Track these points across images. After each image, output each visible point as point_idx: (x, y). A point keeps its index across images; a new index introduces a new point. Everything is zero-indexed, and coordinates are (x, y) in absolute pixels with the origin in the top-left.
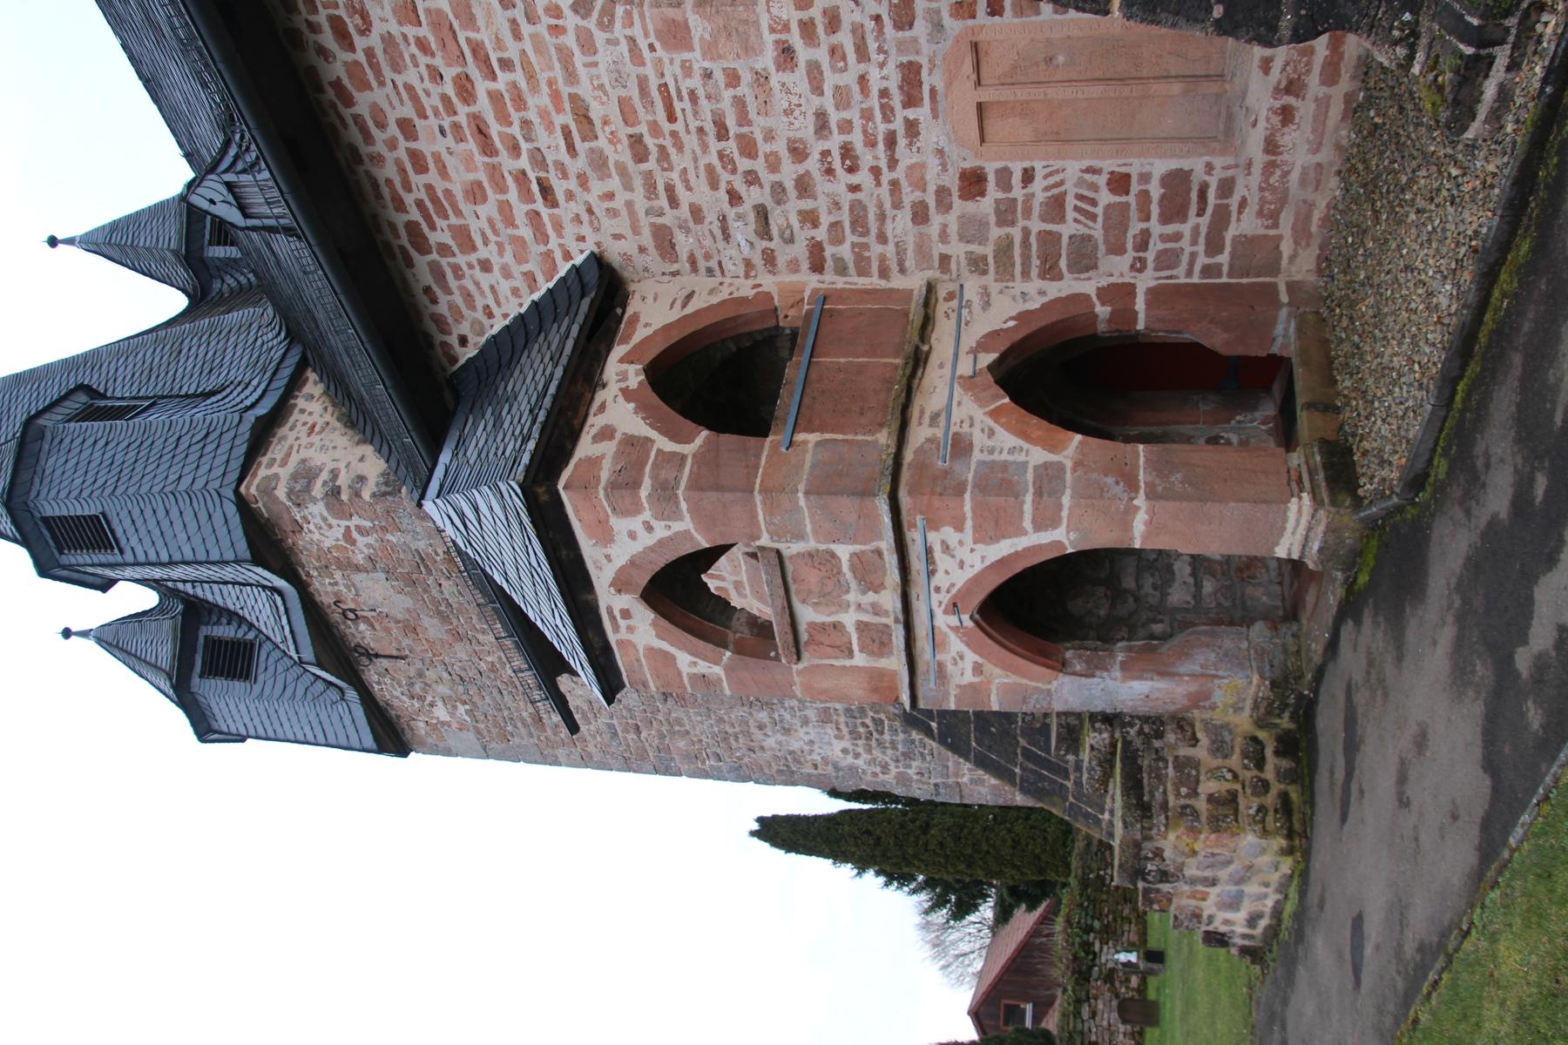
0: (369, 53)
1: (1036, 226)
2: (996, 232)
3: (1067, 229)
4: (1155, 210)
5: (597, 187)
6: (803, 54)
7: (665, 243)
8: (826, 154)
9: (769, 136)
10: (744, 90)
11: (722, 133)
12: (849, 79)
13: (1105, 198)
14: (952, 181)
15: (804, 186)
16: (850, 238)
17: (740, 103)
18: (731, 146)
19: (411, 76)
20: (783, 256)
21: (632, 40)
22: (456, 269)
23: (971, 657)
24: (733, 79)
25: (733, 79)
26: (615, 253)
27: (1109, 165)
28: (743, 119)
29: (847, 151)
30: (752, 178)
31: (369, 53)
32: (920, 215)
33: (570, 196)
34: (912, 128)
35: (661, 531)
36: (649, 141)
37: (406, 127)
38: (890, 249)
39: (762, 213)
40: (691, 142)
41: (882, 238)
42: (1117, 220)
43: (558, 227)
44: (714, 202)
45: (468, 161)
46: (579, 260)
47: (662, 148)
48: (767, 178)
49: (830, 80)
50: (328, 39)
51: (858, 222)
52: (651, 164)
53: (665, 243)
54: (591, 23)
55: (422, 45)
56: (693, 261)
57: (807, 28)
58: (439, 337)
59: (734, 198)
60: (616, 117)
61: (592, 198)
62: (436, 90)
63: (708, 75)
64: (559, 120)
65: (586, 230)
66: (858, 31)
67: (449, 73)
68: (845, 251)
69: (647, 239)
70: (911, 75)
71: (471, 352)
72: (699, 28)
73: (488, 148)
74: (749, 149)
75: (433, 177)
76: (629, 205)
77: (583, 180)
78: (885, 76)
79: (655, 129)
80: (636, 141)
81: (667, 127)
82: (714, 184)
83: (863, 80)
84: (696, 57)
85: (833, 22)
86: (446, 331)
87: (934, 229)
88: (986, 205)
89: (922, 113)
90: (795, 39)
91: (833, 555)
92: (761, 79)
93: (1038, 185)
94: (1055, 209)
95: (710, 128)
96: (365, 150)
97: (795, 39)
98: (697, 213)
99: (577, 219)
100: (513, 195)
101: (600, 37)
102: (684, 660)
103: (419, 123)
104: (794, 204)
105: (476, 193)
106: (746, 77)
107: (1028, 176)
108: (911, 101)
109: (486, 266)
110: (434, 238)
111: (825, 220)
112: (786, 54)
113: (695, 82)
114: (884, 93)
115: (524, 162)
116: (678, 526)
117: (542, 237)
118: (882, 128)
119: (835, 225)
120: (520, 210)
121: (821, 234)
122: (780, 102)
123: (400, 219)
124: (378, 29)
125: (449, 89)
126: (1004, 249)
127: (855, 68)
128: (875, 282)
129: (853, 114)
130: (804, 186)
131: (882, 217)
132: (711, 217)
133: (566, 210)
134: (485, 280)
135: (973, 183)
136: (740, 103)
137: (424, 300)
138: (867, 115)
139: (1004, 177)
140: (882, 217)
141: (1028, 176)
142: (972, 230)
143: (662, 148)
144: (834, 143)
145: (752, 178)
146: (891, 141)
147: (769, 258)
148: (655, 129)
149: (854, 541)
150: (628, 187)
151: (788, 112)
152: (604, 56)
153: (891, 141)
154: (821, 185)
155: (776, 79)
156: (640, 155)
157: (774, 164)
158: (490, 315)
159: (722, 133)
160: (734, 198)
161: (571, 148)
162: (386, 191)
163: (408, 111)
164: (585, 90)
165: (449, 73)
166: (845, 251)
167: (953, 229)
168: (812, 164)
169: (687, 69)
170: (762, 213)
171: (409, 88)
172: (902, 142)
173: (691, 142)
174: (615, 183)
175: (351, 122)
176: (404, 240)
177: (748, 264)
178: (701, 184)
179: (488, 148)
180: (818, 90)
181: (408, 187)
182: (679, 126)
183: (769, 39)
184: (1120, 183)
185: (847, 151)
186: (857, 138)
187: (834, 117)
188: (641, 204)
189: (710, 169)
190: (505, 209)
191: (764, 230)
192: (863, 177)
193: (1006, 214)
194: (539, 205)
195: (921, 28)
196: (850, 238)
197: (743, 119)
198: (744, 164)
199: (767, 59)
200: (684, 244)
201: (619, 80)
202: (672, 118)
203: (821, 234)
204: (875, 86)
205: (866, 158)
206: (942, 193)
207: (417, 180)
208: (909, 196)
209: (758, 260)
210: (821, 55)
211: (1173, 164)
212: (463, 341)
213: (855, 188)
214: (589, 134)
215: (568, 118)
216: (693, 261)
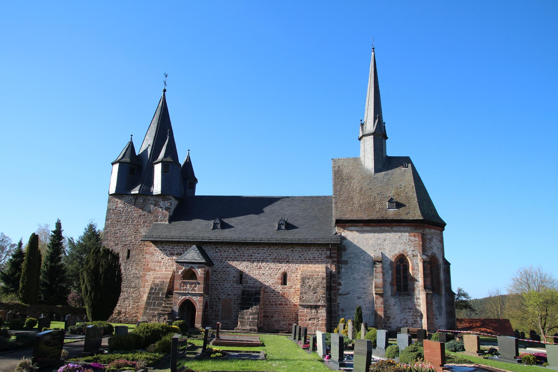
0: (235, 251)
1: (215, 304)
2: (214, 301)
3: (214, 307)
4: (216, 314)
5: (221, 267)
6: (232, 287)
7: (215, 271)
8: (223, 287)
9: (225, 283)
10: (229, 282)
11: (225, 279)
12: (229, 290)
13: (217, 310)
14: (220, 297)
15: (220, 285)
16: (214, 288)
17: (228, 281)
18: (224, 279)
19: (232, 254)
20: (213, 282)
21: (234, 273)
22: (213, 250)
23: (182, 298)
24: (230, 281)
25: (230, 281)
26: (214, 266)
27: (220, 310)
28: (226, 281)
29: (223, 289)
30: (221, 281)
31: (235, 251)
32: (216, 294)
33: (220, 264)
34: (225, 295)
35: (199, 273)
36: (225, 272)
37: (228, 251)
38: (213, 291)
39: (218, 281)
40: (225, 276)
41: (214, 291)
42: (215, 311)
43: (217, 262)
44: (219, 276)
45: (224, 256)
46: (214, 263)
47: (224, 273)
48: (221, 282)
49: (230, 289)
50: (236, 248)
51: (216, 289)
52: (223, 272)
53: (215, 271)
54: (236, 270)
55: (235, 256)
56: (213, 273)
57: (234, 287)
58: (205, 245)
59: (219, 279)
60: (227, 270)
61: (220, 266)
62: (231, 255)
63: (231, 279)
64: (228, 265)
65: (217, 264)
66: (233, 291)
67: (233, 257)
68: (213, 287)
69: (215, 270)
70: (229, 295)
71: (203, 248)
72: (235, 279)
73: (225, 258)
74: (224, 281)
75: (223, 252)
76: (219, 269)
77: (222, 266)
78: (230, 293)
79: (226, 273)
80: (225, 271)
81: (226, 274)
82: (221, 277)
83: (229, 291)
84: (232, 278)
85: (234, 290)
86: (206, 246)
87: (215, 295)
88: (217, 300)
89: (226, 295)
90: (233, 286)
91: (196, 287)
92: (230, 283)
93: (219, 304)
94: (216, 306)
95: (226, 278)
96: (226, 247)
97: (233, 286)
98: (218, 275)
99: (218, 264)
100: (220, 258)
101: (235, 271)
102: (182, 271)
103: (228, 253)
104: (218, 284)
105: (221, 255)
106: (230, 282)
107: (220, 304)
108: (227, 295)
109: (213, 253)
110: (217, 249)
111: (216, 286)
112: (232, 285)
113: (230, 278)
114: (228, 293)
115: (224, 261)
116: (200, 274)
117: (216, 260)
118: (225, 292)
119: (216, 287)
120: (219, 259)
121: (215, 286)
122: (228, 284)
123: (219, 247)
124: (237, 253)
125: (231, 257)
126: (213, 301)
127: (230, 291)
128: (210, 290)
129: (226, 290)
130: (220, 285)
131: (217, 291)
132: (217, 276)
133: (219, 263)
134: (212, 253)
135: (219, 299)
136: (228, 281)
137: (210, 245)
138: (226, 291)
139: (220, 302)
140: (217, 291)
141: (220, 304)
142: (215, 299)
143: (224, 273)
144: (224, 288)
145: (221, 281)
146: (224, 293)
147: (213, 280)
148: (226, 273)
149: (198, 289)
150: (221, 269)
151: (227, 285)
152: (233, 271)
153: (224, 293)
154: (220, 286)
155: (230, 284)
156: (224, 271)
157: (222, 283)
158: (208, 252)
159: (225, 279)
160: (219, 279)
161: (225, 265)
162: (222, 247)
163: (229, 252)
164: (230, 268)
165: (233, 257)
166: (213, 287)
167: (215, 297)
168: (222, 286)
169: (231, 277)
170: (218, 281)
171: (231, 253)
172: (224, 294)
173: (225, 276)
174: (221, 268)
175: (229, 246)
176: (217, 246)
177: (212, 278)
178: (221, 276)
179: (225, 258)
180: (229, 287)
181: (222, 249)
182: (226, 275)
183: (233, 284)
184: (219, 311)
185: (223, 289)
186: (224, 290)
187: (226, 288)
188: (219, 270)
189: (222, 277)
190: (219, 257)
191: (215, 280)
192: (220, 290)
193: (216, 302)
194: (219, 261)
195: (233, 296)
196: (214, 288)
197: (226, 281)
198: (222, 280)
199: (232, 284)
200: (215, 273)
201: (231, 271)
202: (227, 275)
203: (215, 286)
204: (229, 292)
205: (223, 290)
206: (219, 296)
207: (223, 250)
208: (219, 294)
209: (212, 279)
210: (232, 288)
211: (220, 315)
212: (205, 248)
213: (219, 289)
214: (226, 267)
215: (228, 266)
216: (213, 273)
